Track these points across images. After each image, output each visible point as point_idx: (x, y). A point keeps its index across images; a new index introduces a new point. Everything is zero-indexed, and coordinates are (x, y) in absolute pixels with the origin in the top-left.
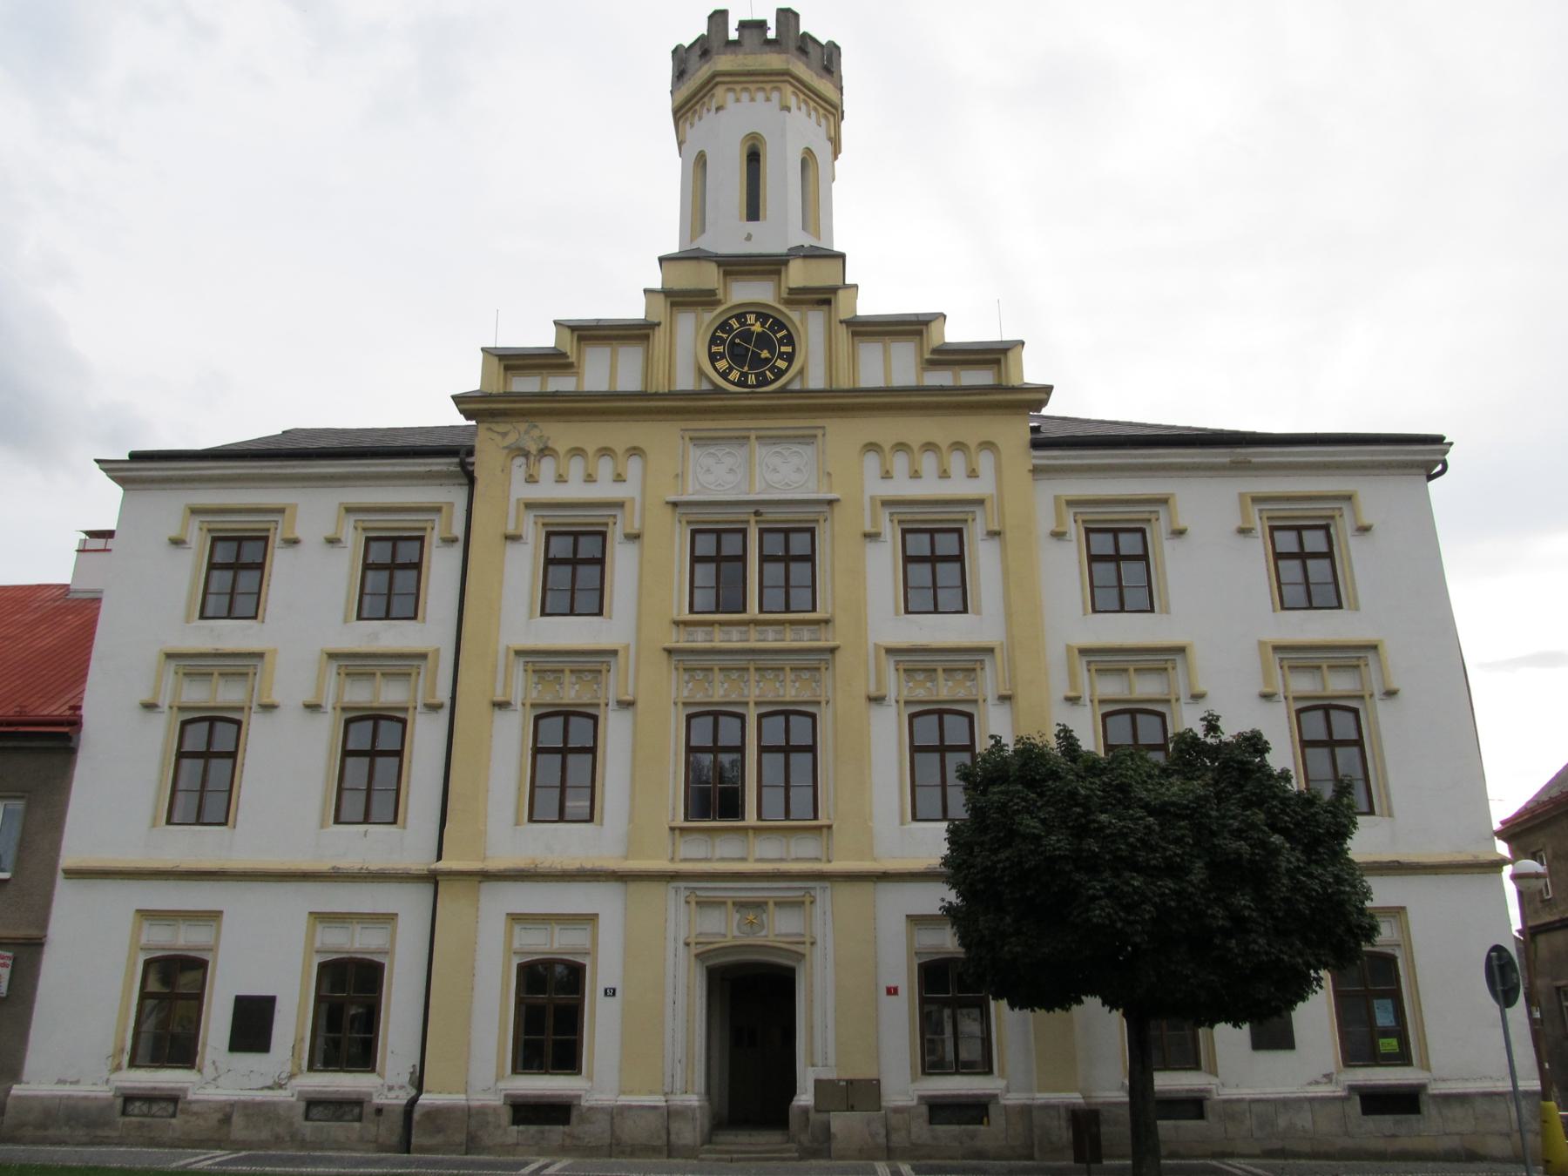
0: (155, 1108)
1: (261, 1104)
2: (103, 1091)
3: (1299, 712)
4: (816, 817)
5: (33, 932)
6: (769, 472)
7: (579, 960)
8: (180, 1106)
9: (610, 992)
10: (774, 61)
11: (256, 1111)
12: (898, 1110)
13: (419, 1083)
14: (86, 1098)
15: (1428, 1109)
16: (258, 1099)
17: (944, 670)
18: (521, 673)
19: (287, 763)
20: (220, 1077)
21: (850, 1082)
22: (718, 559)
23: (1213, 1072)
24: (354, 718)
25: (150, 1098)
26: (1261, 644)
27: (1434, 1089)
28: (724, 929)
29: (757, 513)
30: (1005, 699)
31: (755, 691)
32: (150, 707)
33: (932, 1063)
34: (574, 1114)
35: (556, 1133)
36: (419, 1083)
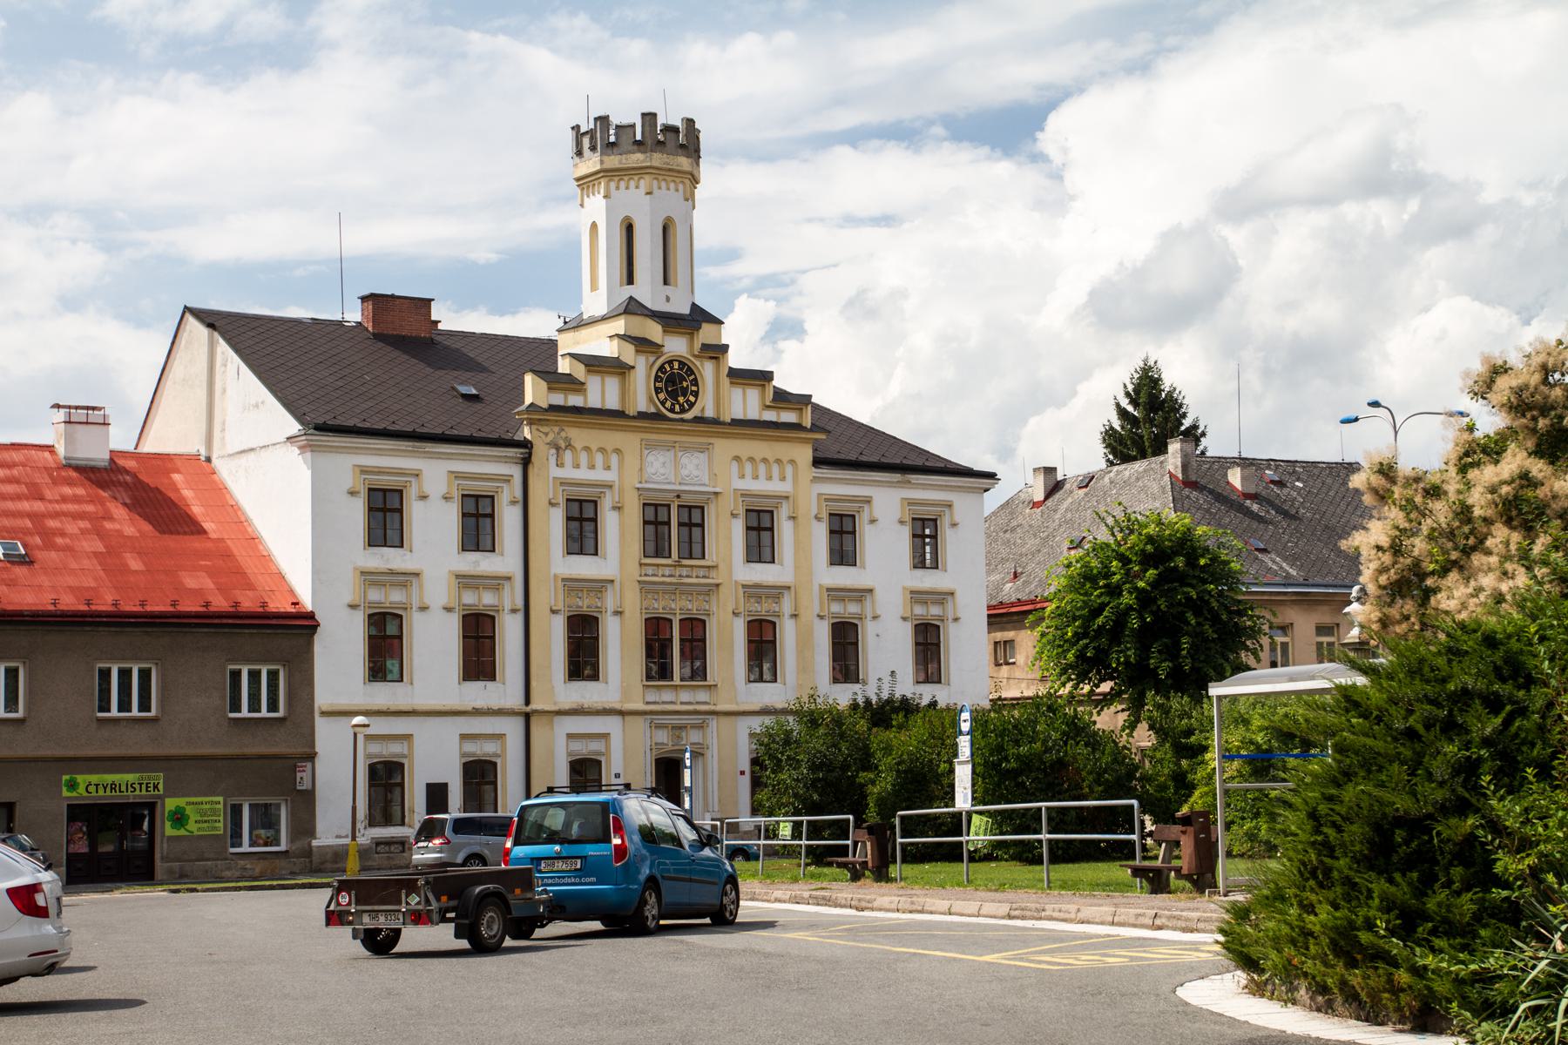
5: (307, 750)
19: (434, 643)
22: (656, 523)
25: (388, 842)
28: (663, 737)
30: (795, 616)
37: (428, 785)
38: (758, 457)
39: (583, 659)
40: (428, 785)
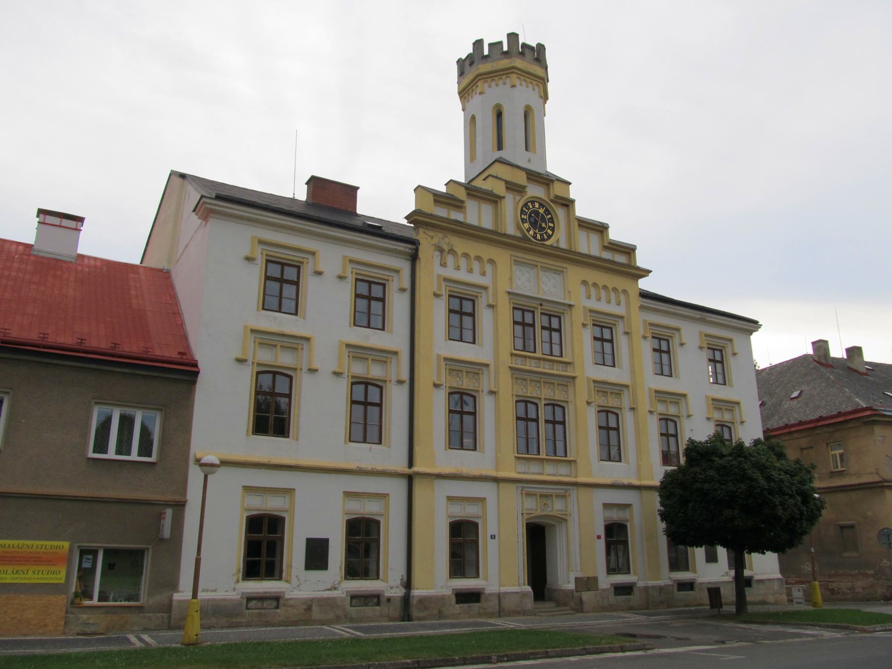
0: (266, 604)
1: (328, 599)
2: (234, 596)
3: (599, 412)
4: (539, 454)
5: (177, 498)
6: (545, 285)
7: (476, 520)
8: (281, 602)
9: (493, 537)
10: (505, 63)
11: (326, 603)
12: (604, 590)
13: (408, 584)
14: (224, 600)
15: (754, 585)
16: (325, 596)
17: (467, 372)
18: (253, 344)
20: (299, 584)
21: (588, 578)
22: (523, 324)
23: (695, 571)
24: (356, 382)
25: (261, 598)
26: (707, 397)
27: (756, 577)
29: (541, 305)
30: (632, 409)
31: (545, 393)
32: (240, 361)
33: (611, 571)
34: (483, 598)
35: (475, 606)
36: (408, 584)
37: (309, 541)
39: (463, 426)
40: (309, 541)
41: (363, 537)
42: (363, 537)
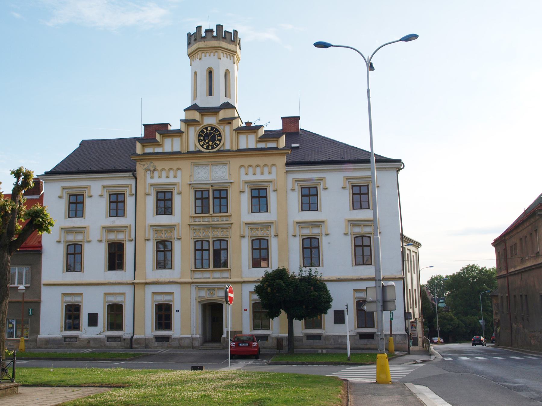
0: (72, 340)
5: (38, 299)
9: (178, 311)
22: (202, 199)
25: (71, 337)
28: (204, 295)
29: (212, 186)
30: (276, 236)
31: (211, 235)
32: (59, 242)
35: (166, 344)
37: (89, 314)
38: (246, 165)
40: (89, 314)
41: (115, 311)
42: (115, 311)
